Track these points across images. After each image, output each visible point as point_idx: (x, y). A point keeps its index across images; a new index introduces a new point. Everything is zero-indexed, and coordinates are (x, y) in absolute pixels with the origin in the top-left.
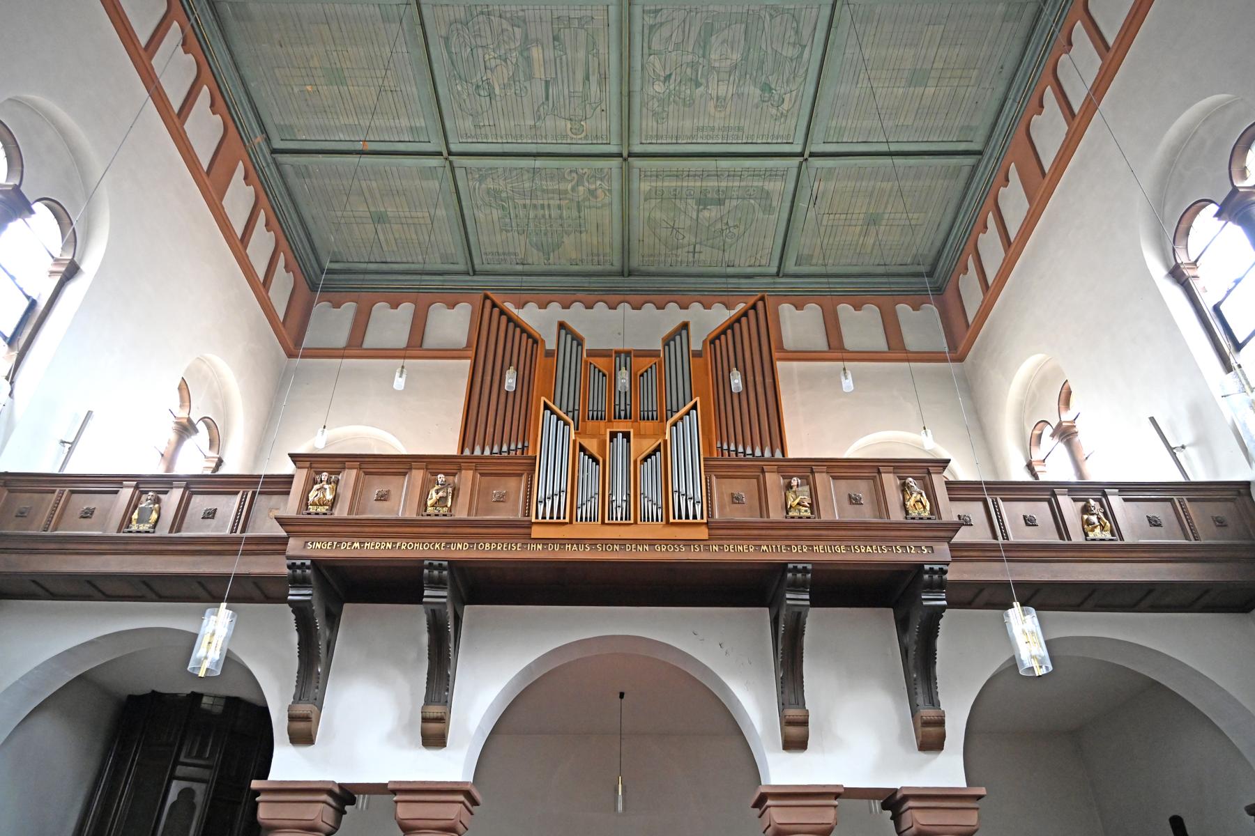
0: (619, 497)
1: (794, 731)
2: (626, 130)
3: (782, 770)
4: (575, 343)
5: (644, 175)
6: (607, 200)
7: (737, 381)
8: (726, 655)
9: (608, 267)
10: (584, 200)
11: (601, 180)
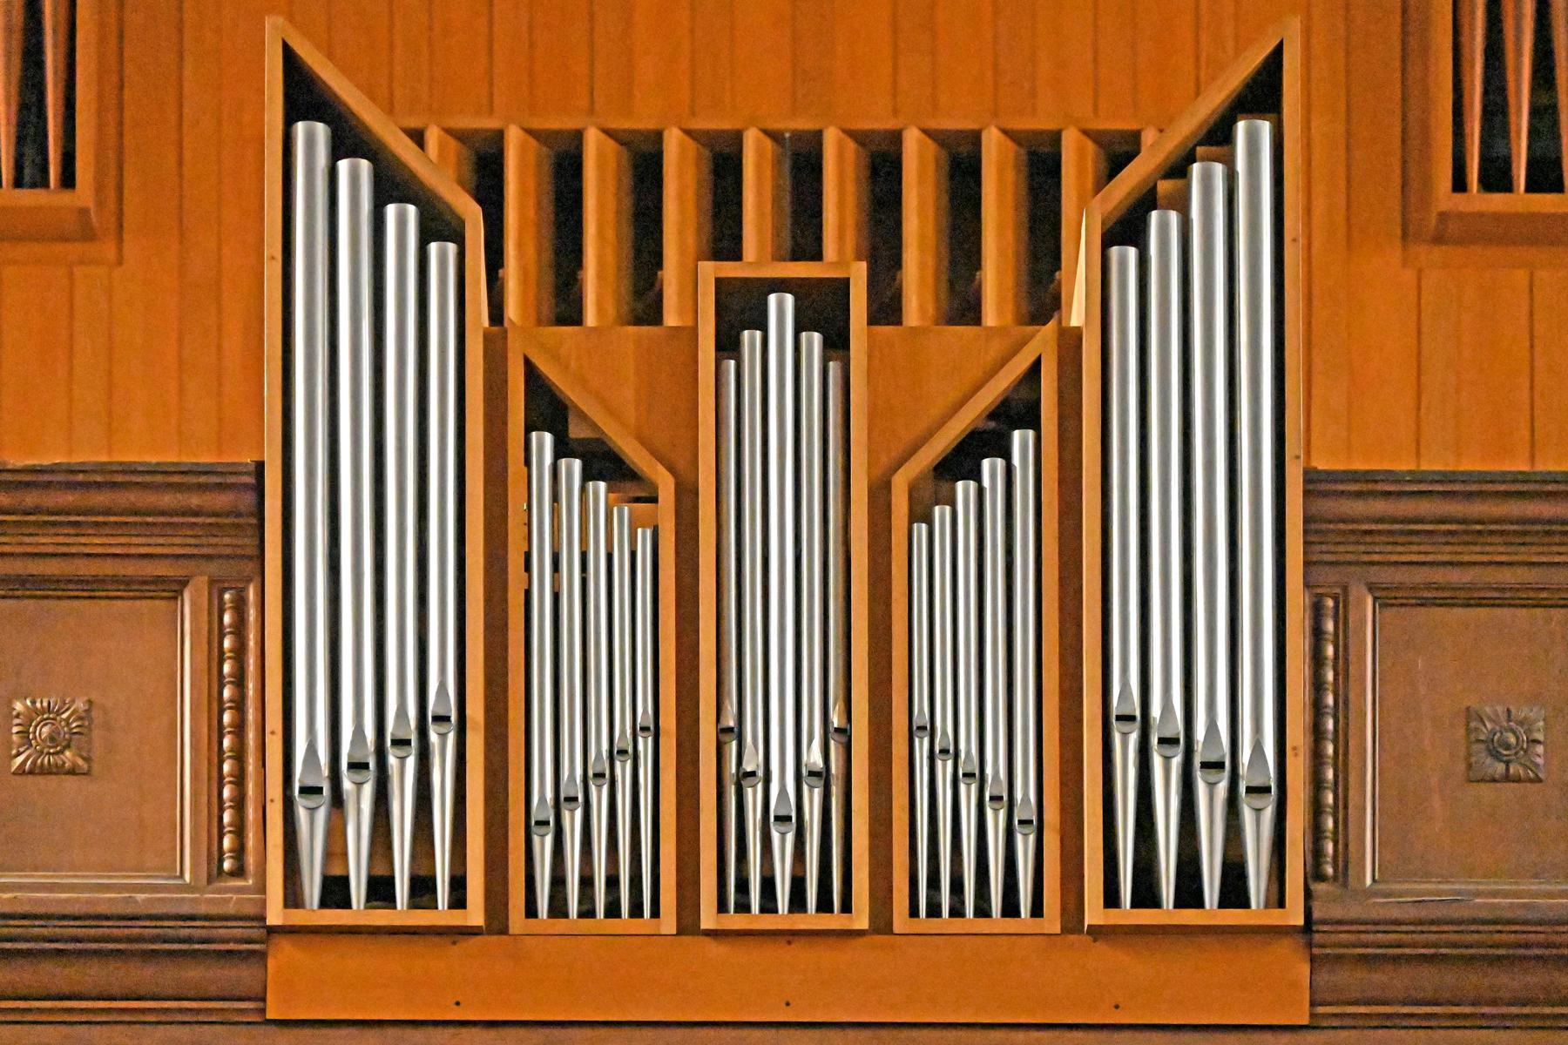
0: (784, 735)
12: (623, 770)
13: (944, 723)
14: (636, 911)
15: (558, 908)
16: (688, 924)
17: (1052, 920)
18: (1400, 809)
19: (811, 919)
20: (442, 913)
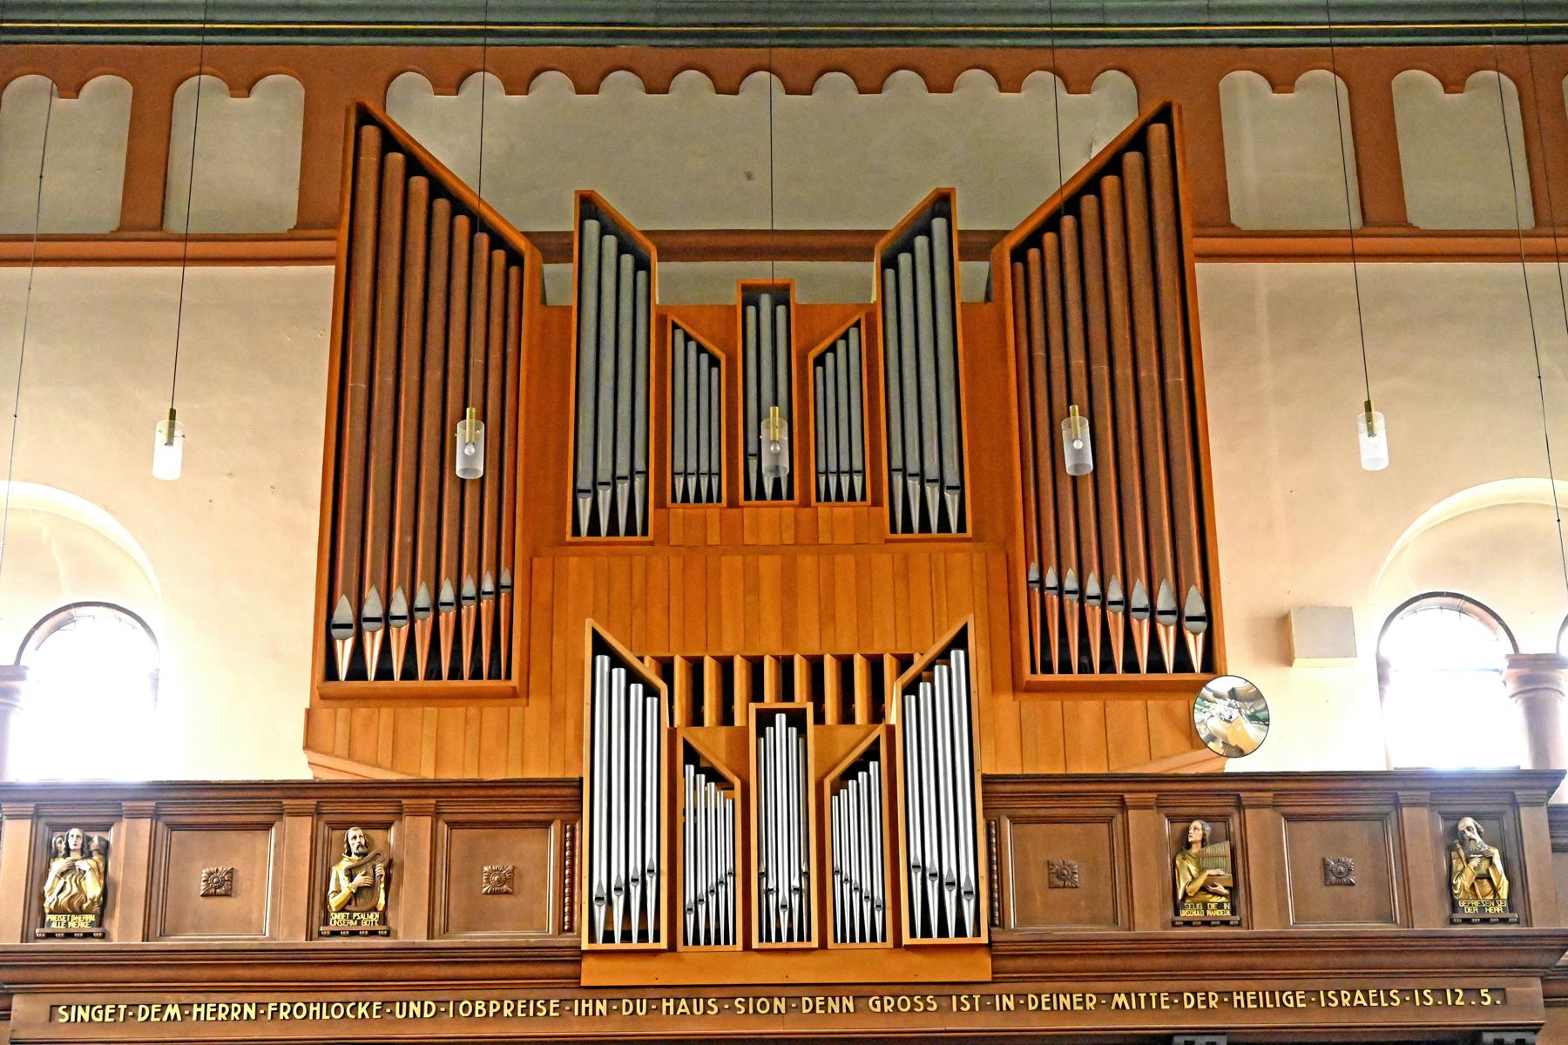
0: (784, 876)
4: (627, 260)
7: (1077, 446)
12: (721, 890)
13: (846, 869)
14: (727, 942)
15: (696, 941)
16: (747, 946)
17: (890, 943)
18: (1023, 898)
19: (796, 944)
20: (650, 945)
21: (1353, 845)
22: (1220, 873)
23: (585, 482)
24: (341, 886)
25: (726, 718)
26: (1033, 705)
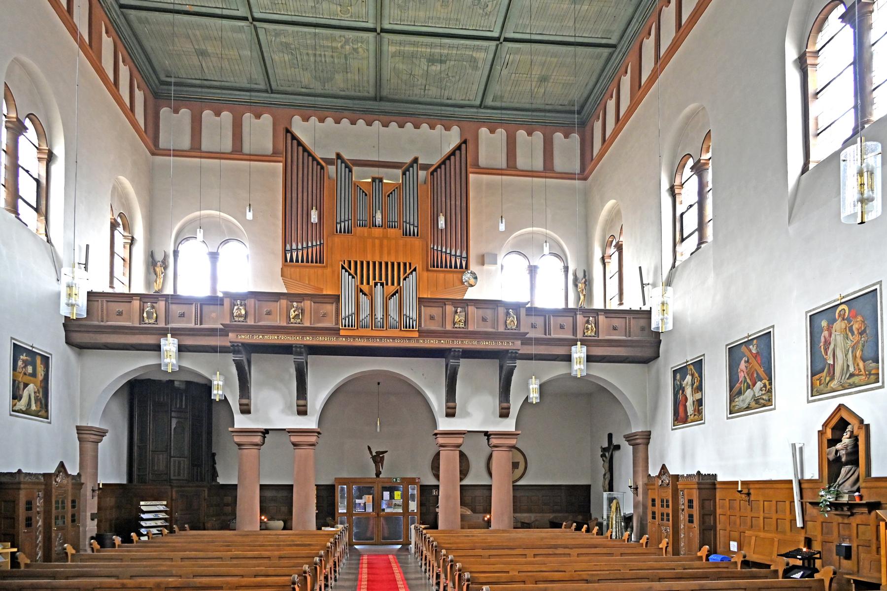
0: (379, 315)
1: (450, 411)
2: (380, 14)
3: (444, 424)
5: (391, 43)
6: (366, 55)
8: (426, 378)
9: (366, 94)
10: (349, 54)
11: (362, 42)
21: (489, 313)
22: (463, 318)
23: (338, 221)
24: (292, 314)
25: (368, 283)
26: (430, 274)
